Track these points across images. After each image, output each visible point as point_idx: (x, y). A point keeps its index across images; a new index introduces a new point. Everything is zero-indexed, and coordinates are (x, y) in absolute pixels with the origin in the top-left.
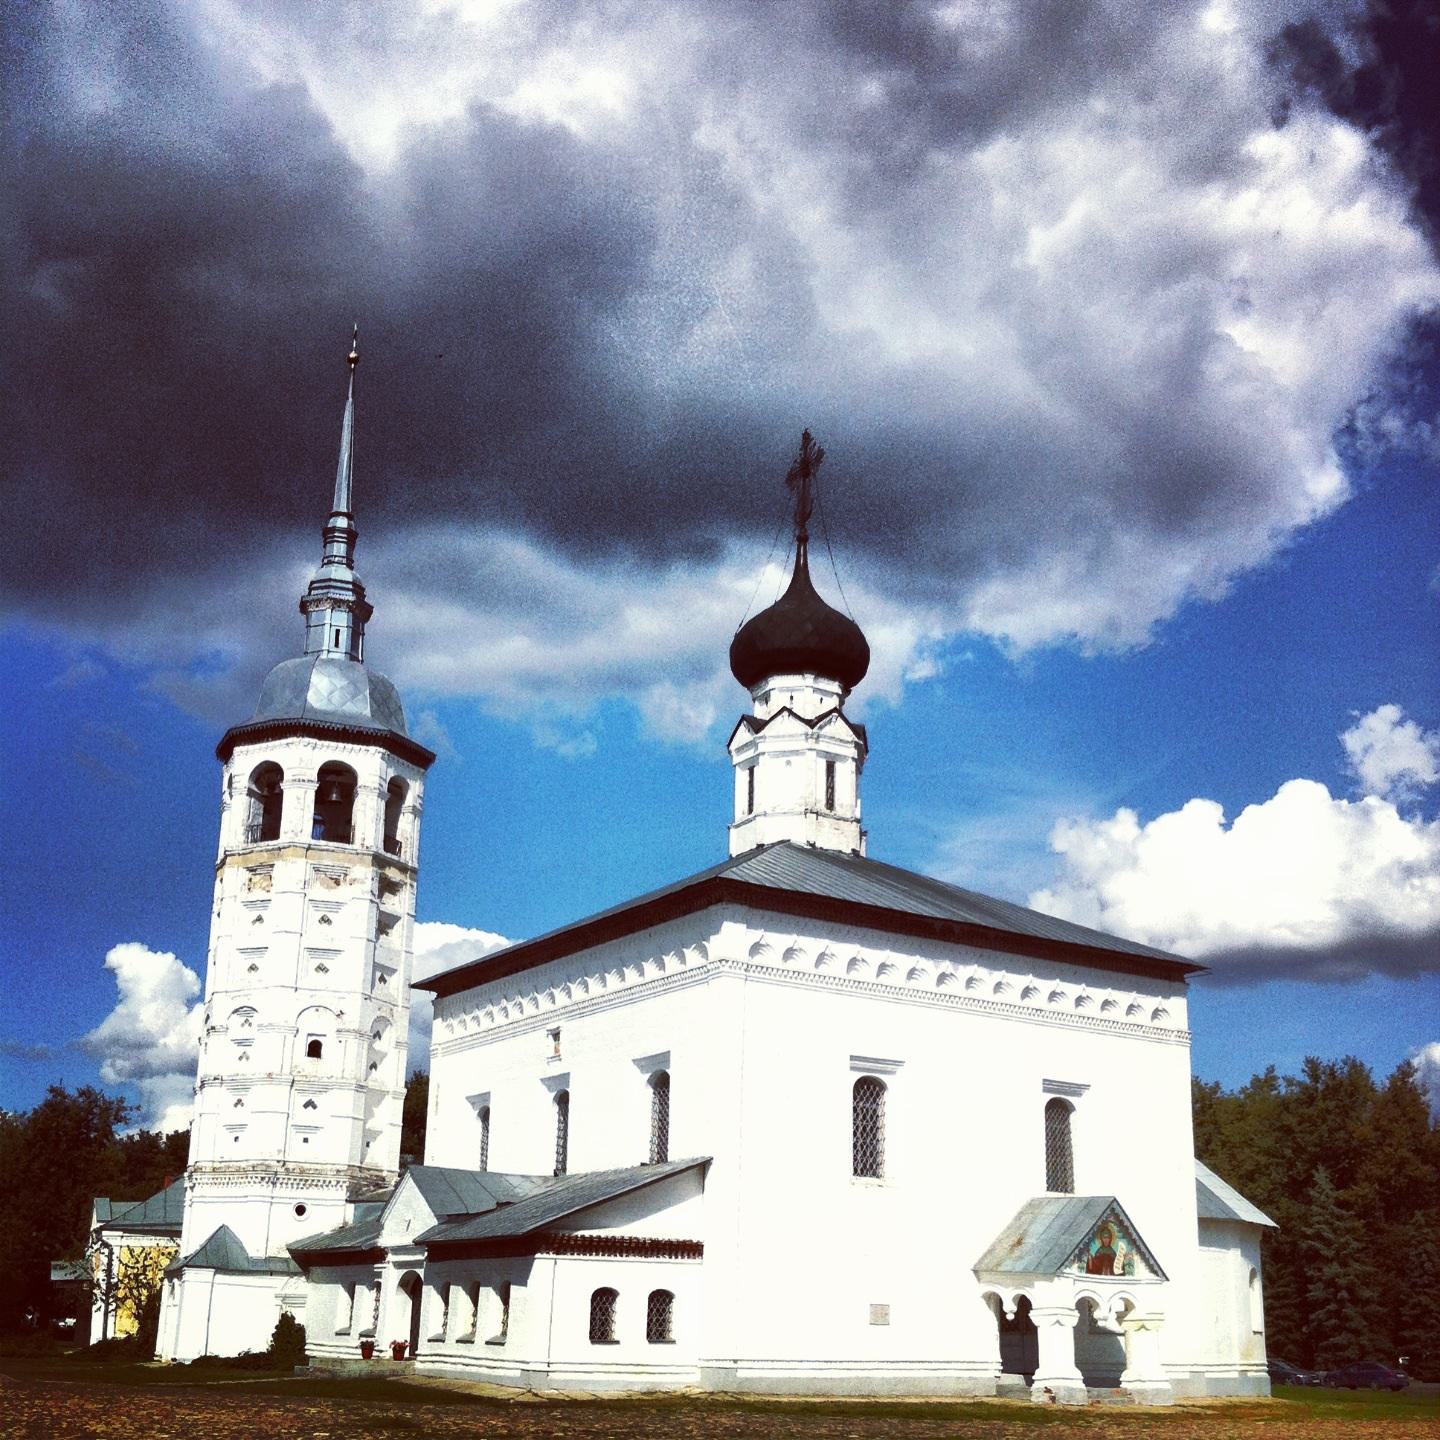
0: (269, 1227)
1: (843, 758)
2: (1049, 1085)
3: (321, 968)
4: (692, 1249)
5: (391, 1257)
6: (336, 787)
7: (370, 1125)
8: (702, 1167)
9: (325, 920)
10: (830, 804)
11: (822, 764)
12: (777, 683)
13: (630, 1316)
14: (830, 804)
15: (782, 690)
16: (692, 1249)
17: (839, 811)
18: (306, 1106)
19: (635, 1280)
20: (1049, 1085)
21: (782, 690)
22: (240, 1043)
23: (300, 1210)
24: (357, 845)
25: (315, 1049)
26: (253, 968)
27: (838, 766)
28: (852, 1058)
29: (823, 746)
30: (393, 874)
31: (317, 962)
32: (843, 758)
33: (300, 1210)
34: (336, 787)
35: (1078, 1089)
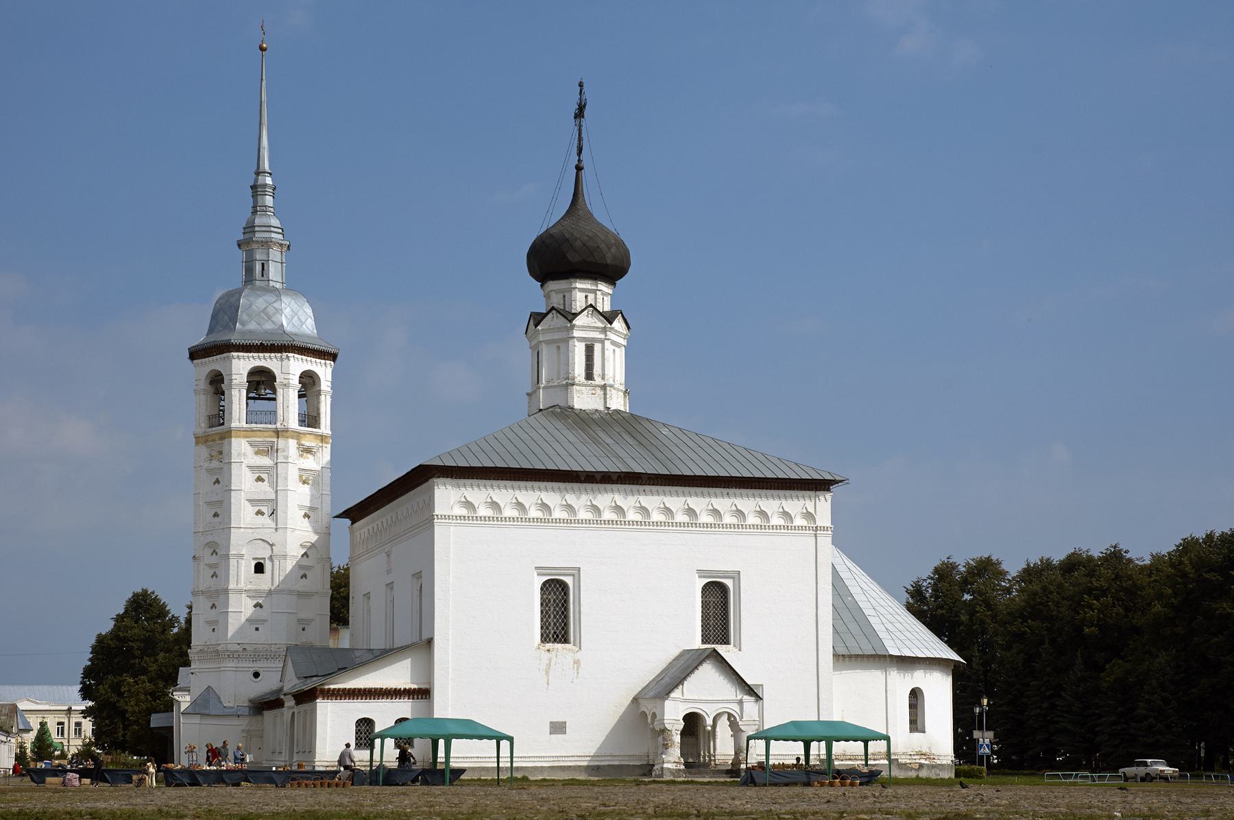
0: (238, 687)
2: (702, 573)
3: (260, 513)
5: (286, 704)
6: (262, 382)
7: (303, 616)
8: (430, 642)
9: (260, 479)
10: (589, 376)
12: (553, 285)
14: (589, 376)
15: (557, 292)
18: (255, 606)
20: (702, 573)
21: (557, 292)
22: (210, 566)
23: (256, 675)
24: (278, 425)
25: (259, 568)
26: (216, 515)
28: (537, 568)
30: (307, 442)
31: (257, 509)
33: (256, 675)
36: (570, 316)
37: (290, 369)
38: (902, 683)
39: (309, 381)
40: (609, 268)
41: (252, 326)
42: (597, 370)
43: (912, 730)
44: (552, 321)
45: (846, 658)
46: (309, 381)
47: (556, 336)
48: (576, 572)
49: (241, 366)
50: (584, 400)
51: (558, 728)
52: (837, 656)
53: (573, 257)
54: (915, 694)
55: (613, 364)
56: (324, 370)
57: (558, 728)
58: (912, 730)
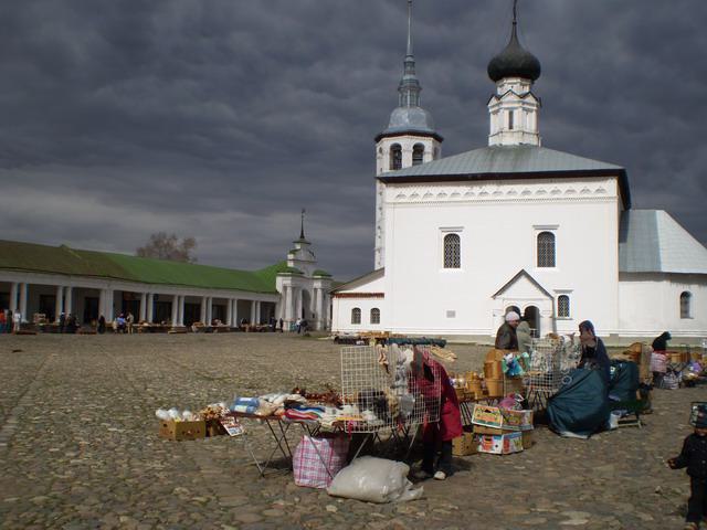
1: (516, 108)
2: (536, 227)
4: (381, 295)
6: (396, 150)
8: (383, 269)
10: (511, 127)
11: (507, 112)
13: (366, 316)
14: (511, 127)
16: (381, 295)
17: (515, 129)
19: (366, 306)
27: (515, 112)
29: (506, 106)
32: (516, 108)
34: (396, 150)
35: (555, 227)
36: (499, 98)
37: (407, 143)
38: (678, 289)
39: (418, 150)
40: (529, 71)
41: (395, 126)
42: (515, 123)
43: (682, 317)
44: (494, 101)
45: (624, 276)
46: (418, 150)
47: (497, 108)
48: (460, 229)
49: (387, 144)
50: (510, 140)
51: (451, 314)
52: (620, 273)
53: (501, 67)
54: (685, 295)
55: (528, 121)
56: (428, 143)
57: (451, 314)
58: (682, 317)
